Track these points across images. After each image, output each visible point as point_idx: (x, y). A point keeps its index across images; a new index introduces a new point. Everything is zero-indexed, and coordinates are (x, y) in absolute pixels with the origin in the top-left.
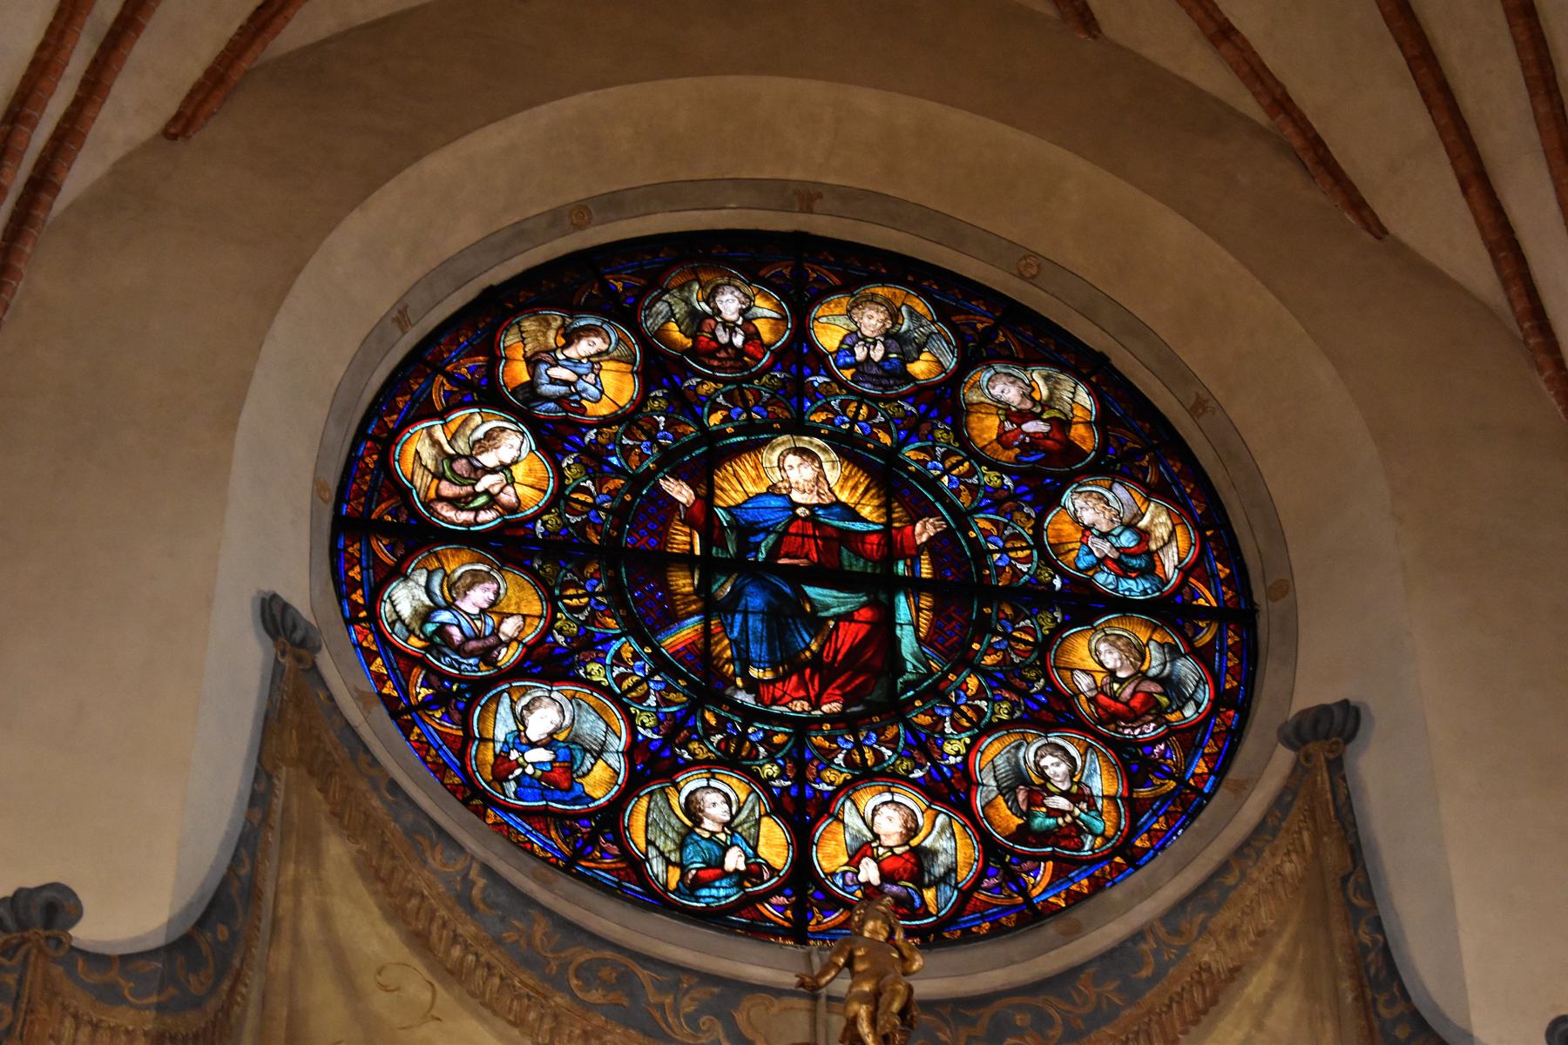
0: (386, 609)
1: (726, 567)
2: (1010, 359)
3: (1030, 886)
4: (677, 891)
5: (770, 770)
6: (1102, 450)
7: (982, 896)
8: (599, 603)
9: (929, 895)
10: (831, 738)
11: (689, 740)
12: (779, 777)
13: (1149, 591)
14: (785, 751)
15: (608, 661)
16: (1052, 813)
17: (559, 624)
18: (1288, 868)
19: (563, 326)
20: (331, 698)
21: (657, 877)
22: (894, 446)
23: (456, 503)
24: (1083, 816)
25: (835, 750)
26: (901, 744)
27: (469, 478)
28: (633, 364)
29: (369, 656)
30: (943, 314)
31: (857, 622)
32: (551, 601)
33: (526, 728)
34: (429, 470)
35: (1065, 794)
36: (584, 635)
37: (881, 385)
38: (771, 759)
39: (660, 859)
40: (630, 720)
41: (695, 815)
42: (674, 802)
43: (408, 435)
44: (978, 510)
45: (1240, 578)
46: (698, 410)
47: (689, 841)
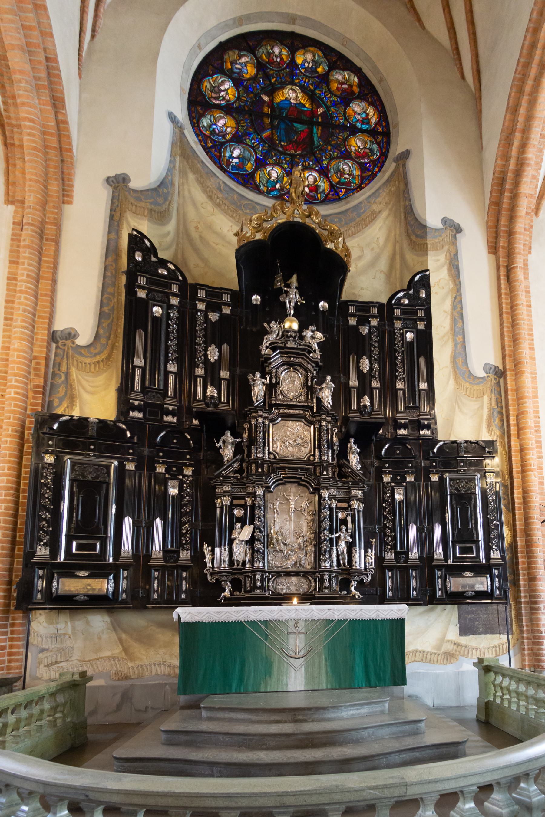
0: (201, 124)
23: (216, 99)
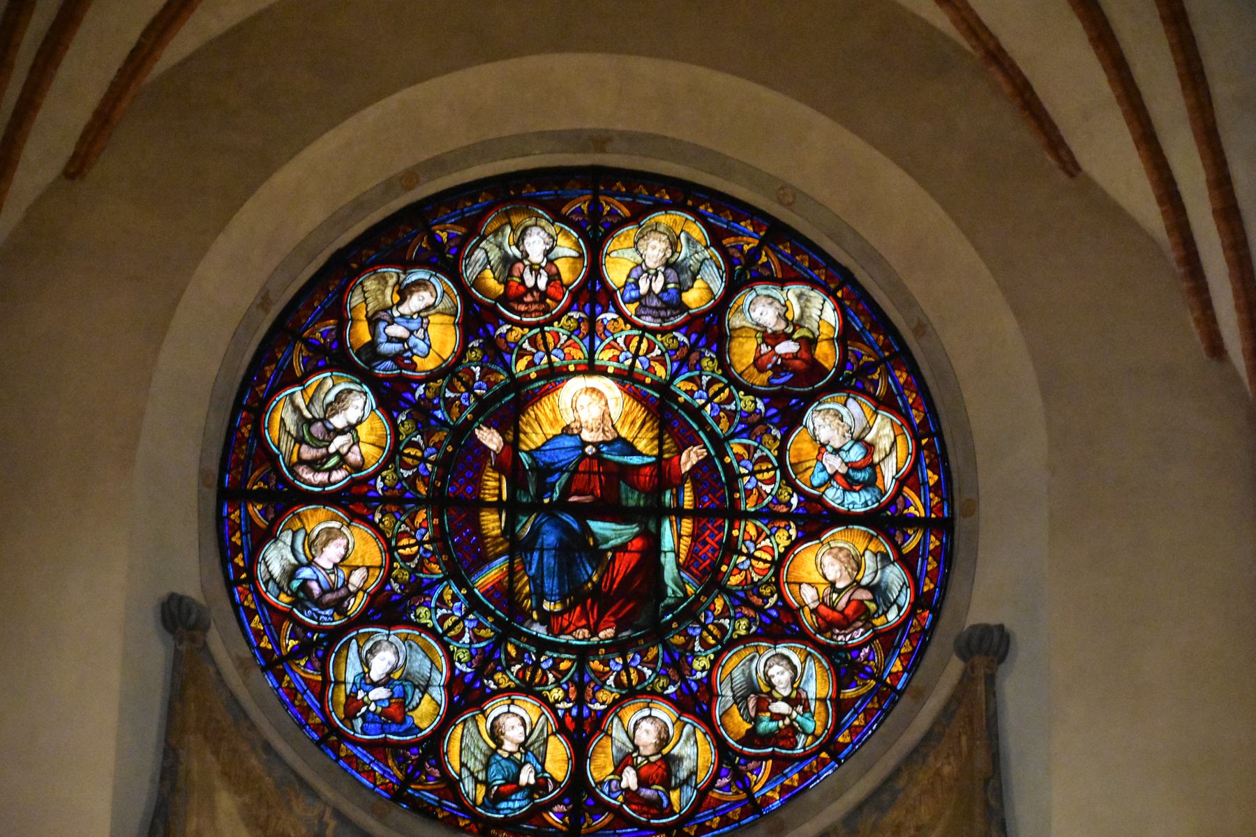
0: (261, 569)
1: (528, 509)
2: (771, 280)
3: (753, 783)
4: (483, 805)
5: (557, 694)
6: (841, 367)
7: (716, 794)
8: (426, 551)
9: (674, 796)
10: (605, 663)
11: (495, 671)
12: (564, 700)
13: (870, 503)
14: (569, 676)
15: (433, 605)
16: (776, 717)
17: (394, 573)
18: (947, 770)
19: (398, 283)
20: (218, 673)
21: (468, 795)
22: (668, 378)
23: (315, 465)
24: (799, 718)
25: (607, 672)
26: (659, 664)
27: (323, 440)
28: (455, 316)
29: (251, 614)
30: (716, 237)
31: (631, 551)
32: (390, 551)
33: (370, 670)
34: (292, 436)
35: (786, 699)
36: (414, 582)
37: (659, 317)
38: (558, 683)
39: (470, 778)
40: (449, 656)
41: (498, 737)
42: (482, 728)
43: (274, 403)
44: (733, 436)
45: (945, 488)
46: (507, 357)
47: (493, 761)
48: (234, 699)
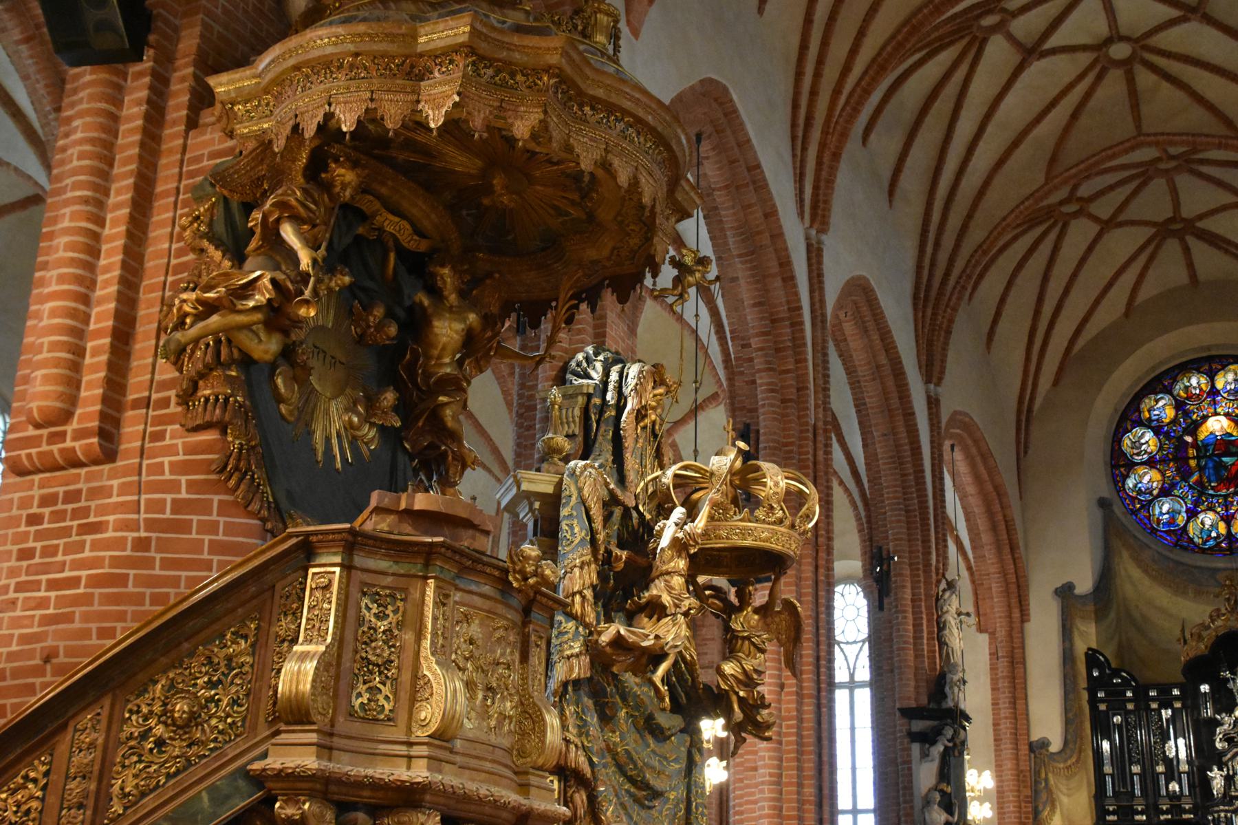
1: (1203, 457)
5: (1219, 509)
23: (1138, 454)
32: (1163, 475)
40: (1185, 503)
48: (1122, 524)
